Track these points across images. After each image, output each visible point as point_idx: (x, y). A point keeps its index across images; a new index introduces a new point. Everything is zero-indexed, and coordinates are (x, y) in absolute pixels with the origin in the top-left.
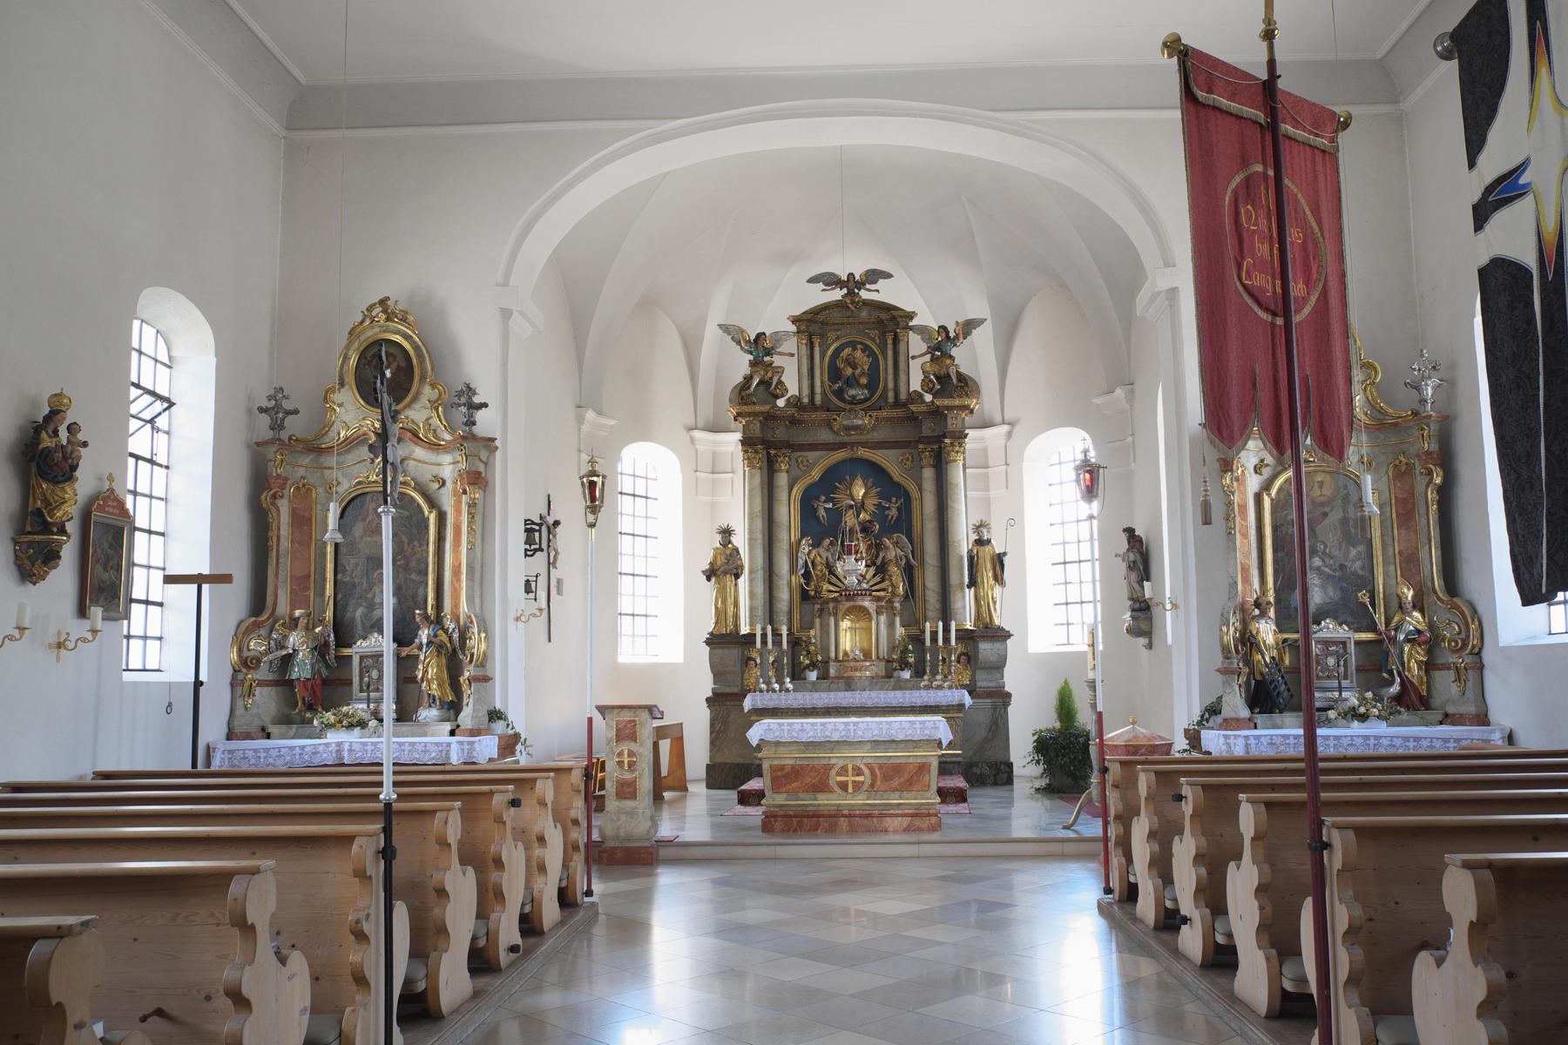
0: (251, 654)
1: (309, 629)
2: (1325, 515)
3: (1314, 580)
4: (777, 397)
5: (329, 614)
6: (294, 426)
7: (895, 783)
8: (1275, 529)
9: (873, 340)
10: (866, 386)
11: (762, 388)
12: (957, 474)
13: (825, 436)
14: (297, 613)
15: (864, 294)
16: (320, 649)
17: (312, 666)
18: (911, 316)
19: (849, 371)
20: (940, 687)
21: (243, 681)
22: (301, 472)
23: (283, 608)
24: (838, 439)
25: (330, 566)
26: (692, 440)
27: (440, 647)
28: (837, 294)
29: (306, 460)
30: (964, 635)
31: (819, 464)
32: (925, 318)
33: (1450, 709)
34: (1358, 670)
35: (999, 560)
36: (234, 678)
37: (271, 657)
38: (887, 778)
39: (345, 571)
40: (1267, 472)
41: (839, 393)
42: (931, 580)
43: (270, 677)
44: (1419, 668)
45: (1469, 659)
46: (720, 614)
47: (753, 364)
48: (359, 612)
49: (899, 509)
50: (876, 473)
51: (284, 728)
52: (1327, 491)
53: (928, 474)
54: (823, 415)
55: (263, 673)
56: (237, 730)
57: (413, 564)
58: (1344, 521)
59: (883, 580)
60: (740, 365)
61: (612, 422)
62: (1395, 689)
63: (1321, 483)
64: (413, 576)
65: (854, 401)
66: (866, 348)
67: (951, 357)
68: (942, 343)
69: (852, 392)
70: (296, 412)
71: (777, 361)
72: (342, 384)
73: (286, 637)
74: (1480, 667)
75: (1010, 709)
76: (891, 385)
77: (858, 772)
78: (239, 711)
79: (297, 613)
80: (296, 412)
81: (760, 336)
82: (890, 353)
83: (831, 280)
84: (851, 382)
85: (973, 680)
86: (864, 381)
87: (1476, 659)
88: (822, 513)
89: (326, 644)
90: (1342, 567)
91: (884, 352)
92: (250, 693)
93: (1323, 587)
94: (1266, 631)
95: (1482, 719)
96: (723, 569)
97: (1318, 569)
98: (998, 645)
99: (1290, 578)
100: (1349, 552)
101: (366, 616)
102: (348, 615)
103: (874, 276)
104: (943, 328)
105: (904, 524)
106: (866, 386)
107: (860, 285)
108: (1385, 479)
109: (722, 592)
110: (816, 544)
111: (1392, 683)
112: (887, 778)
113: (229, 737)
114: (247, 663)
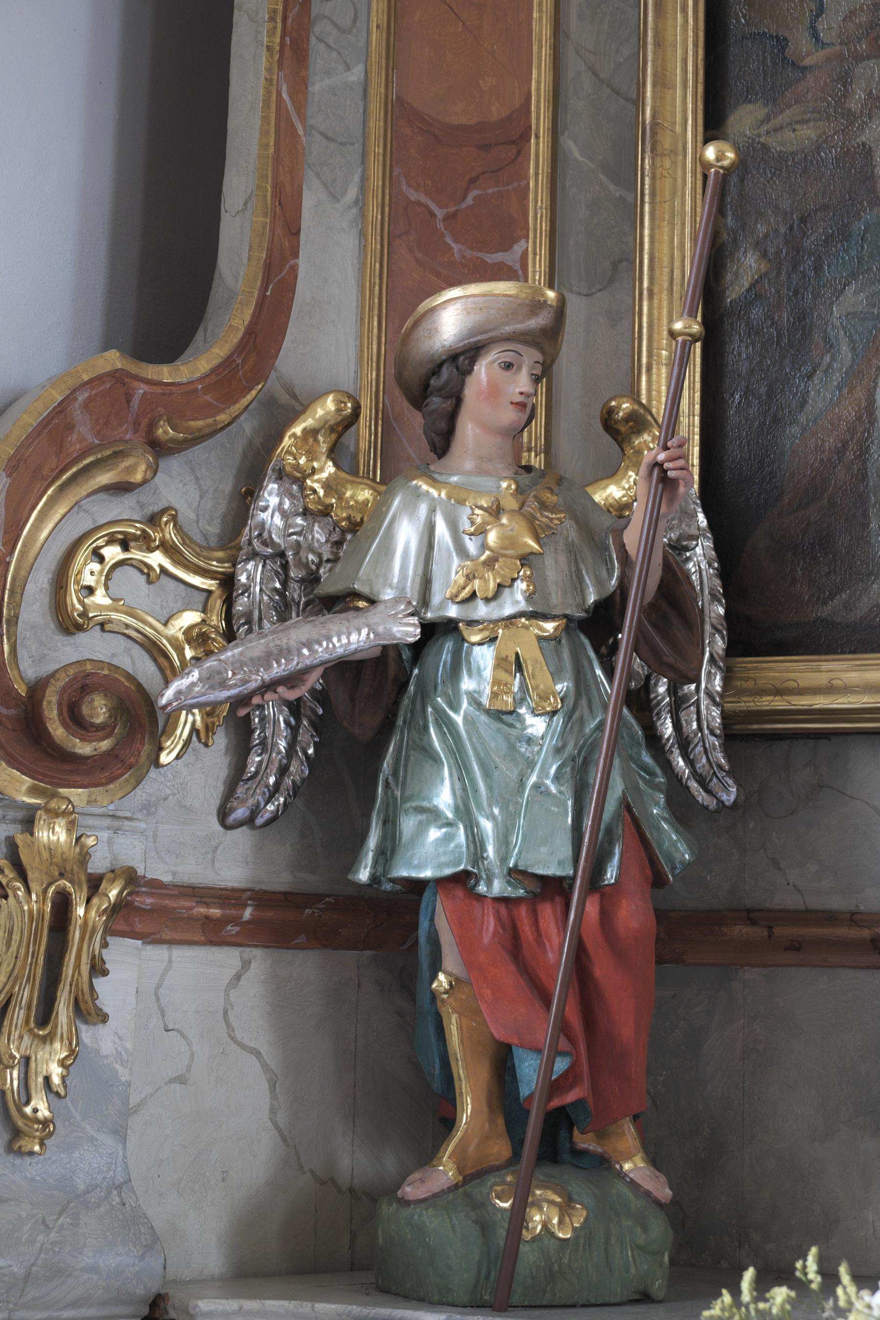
1: (543, 482)
5: (666, 385)
14: (451, 317)
17: (578, 773)
23: (330, 348)
37: (242, 665)
43: (231, 862)
55: (177, 821)
73: (354, 532)
79: (451, 317)
89: (673, 592)
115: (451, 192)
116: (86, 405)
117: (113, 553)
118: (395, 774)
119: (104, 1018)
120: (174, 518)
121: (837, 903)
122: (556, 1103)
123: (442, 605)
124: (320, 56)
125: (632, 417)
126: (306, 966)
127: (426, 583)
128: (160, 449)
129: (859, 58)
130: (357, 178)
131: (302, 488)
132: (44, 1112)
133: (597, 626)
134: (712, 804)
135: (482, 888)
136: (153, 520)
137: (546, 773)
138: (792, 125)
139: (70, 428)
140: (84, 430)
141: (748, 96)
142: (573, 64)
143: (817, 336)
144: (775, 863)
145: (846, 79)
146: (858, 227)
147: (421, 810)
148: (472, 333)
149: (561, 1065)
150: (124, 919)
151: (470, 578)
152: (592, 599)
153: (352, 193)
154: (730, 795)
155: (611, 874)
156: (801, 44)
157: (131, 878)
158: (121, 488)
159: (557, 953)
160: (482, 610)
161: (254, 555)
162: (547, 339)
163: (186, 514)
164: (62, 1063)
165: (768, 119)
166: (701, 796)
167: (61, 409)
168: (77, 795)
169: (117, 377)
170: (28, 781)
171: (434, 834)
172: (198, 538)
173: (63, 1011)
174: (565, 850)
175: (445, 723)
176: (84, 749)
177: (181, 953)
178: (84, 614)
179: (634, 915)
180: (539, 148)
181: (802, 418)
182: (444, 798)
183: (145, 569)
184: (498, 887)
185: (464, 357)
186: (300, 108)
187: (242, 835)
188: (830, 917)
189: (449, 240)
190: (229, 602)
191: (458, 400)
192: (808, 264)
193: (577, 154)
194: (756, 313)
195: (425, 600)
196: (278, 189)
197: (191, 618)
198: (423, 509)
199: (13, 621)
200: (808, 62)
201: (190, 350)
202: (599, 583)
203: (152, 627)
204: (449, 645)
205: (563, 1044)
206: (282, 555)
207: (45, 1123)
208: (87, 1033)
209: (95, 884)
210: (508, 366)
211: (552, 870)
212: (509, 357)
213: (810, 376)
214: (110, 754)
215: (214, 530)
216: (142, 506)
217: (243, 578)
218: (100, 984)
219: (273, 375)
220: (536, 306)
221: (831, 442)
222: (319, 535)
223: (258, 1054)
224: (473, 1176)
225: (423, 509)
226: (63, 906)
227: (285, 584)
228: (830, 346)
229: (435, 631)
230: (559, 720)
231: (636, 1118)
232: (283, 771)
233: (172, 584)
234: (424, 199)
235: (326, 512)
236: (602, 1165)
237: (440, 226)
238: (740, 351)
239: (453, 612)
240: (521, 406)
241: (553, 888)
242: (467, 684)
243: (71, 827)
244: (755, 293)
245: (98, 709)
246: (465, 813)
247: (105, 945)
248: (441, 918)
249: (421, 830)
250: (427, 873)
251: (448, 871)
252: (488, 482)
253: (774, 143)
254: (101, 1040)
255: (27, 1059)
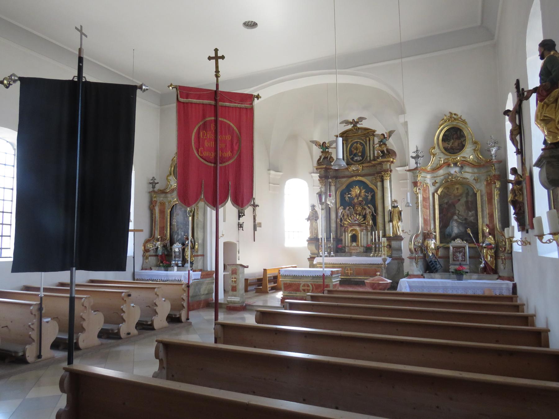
2: (459, 200)
3: (455, 224)
4: (331, 162)
5: (168, 237)
6: (157, 187)
7: (319, 290)
8: (440, 206)
9: (363, 140)
10: (361, 156)
11: (326, 160)
12: (387, 184)
15: (359, 126)
16: (165, 246)
18: (374, 131)
19: (355, 151)
20: (377, 256)
22: (162, 199)
25: (169, 224)
26: (312, 177)
28: (350, 127)
29: (163, 195)
30: (389, 239)
31: (345, 182)
32: (379, 132)
33: (501, 274)
34: (469, 258)
35: (400, 213)
38: (317, 288)
40: (437, 185)
41: (352, 159)
42: (380, 220)
43: (154, 254)
44: (491, 257)
45: (506, 255)
46: (311, 232)
47: (322, 152)
49: (372, 196)
50: (362, 184)
52: (460, 191)
53: (379, 184)
55: (152, 253)
58: (467, 202)
59: (364, 220)
60: (317, 152)
61: (281, 174)
62: (482, 265)
63: (457, 189)
65: (357, 161)
66: (361, 143)
67: (386, 145)
68: (383, 139)
69: (355, 158)
70: (158, 183)
71: (330, 150)
72: (171, 174)
74: (511, 259)
75: (404, 264)
76: (368, 155)
77: (308, 286)
78: (145, 263)
80: (158, 183)
81: (324, 143)
82: (368, 144)
83: (347, 122)
84: (355, 155)
85: (391, 254)
86: (360, 154)
87: (509, 255)
88: (347, 198)
90: (466, 219)
91: (366, 144)
92: (147, 258)
93: (458, 227)
94: (432, 244)
95: (511, 279)
96: (313, 217)
97: (456, 220)
98: (398, 242)
99: (444, 224)
100: (468, 213)
103: (361, 119)
104: (383, 135)
105: (373, 201)
106: (361, 156)
107: (357, 122)
108: (483, 185)
109: (311, 224)
110: (344, 209)
111: (481, 263)
112: (317, 288)
113: (142, 269)
114: (146, 251)
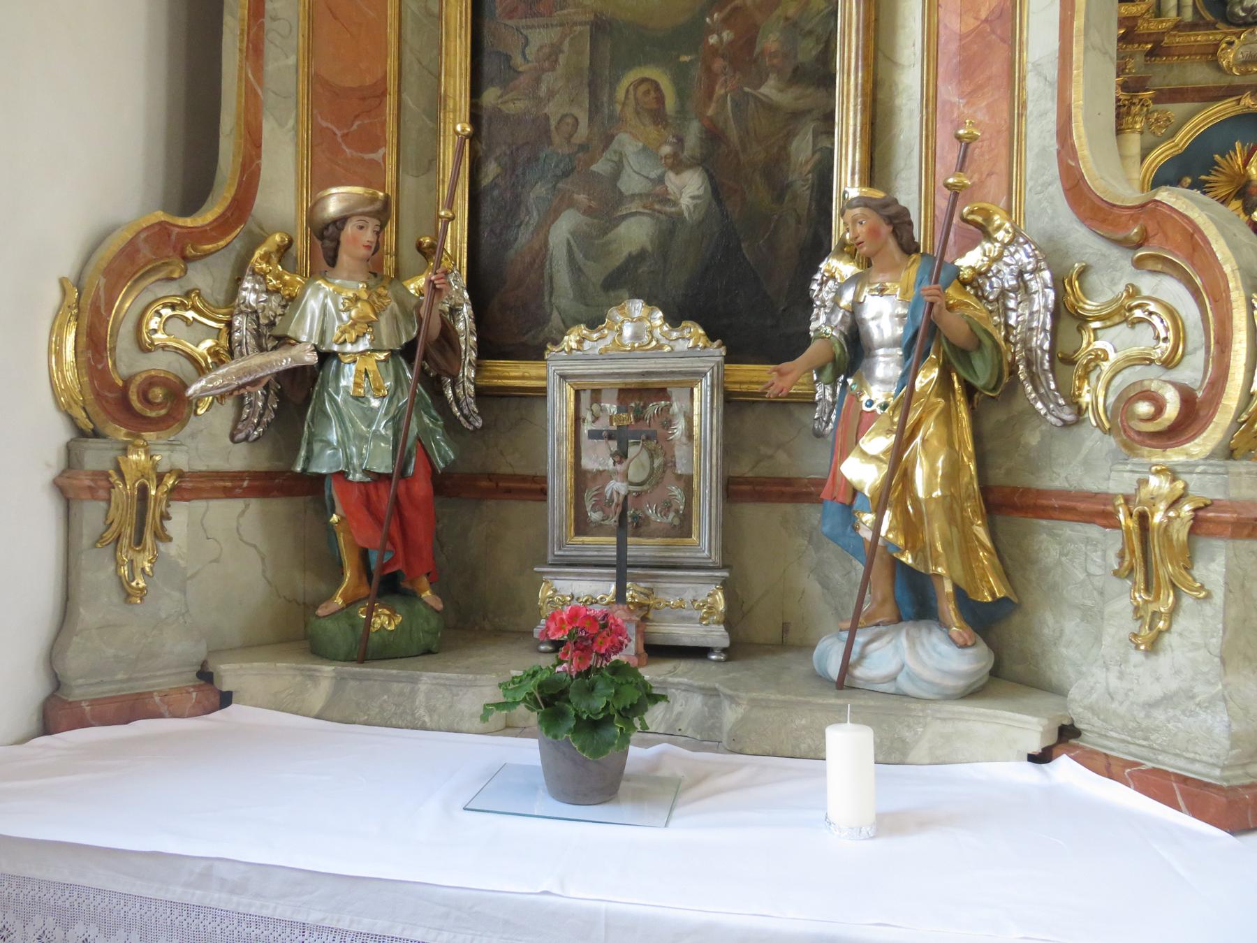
0: (159, 363)
13: (1200, 75)
14: (335, 202)
16: (424, 358)
21: (102, 484)
24: (1224, 81)
27: (956, 358)
36: (71, 457)
39: (509, 73)
43: (238, 459)
48: (563, 229)
51: (283, 673)
54: (1201, 37)
55: (210, 440)
56: (81, 691)
57: (771, 41)
64: (770, 89)
73: (292, 302)
89: (447, 337)
92: (143, 523)
101: (588, 245)
102: (524, 238)
115: (347, 121)
116: (146, 240)
117: (167, 312)
118: (312, 421)
119: (170, 539)
120: (199, 295)
121: (529, 472)
122: (388, 571)
123: (331, 344)
124: (270, 51)
125: (432, 246)
126: (279, 506)
127: (323, 333)
128: (186, 259)
129: (544, 71)
130: (293, 115)
131: (265, 279)
132: (142, 584)
133: (408, 352)
134: (471, 428)
135: (351, 477)
136: (187, 295)
137: (382, 426)
138: (513, 100)
139: (138, 251)
140: (146, 252)
141: (492, 83)
142: (408, 57)
143: (523, 209)
144: (502, 453)
145: (538, 80)
146: (542, 155)
147: (322, 441)
148: (342, 211)
149: (388, 557)
150: (177, 493)
151: (343, 332)
152: (404, 341)
153: (291, 122)
154: (479, 424)
155: (411, 470)
156: (518, 60)
157: (181, 475)
158: (170, 279)
159: (385, 505)
160: (349, 348)
161: (241, 312)
162: (382, 213)
163: (206, 291)
164: (150, 562)
165: (501, 97)
166: (466, 425)
167: (132, 242)
168: (150, 436)
169: (161, 224)
170: (124, 430)
171: (329, 452)
172: (212, 302)
173: (149, 538)
174: (389, 461)
175: (333, 400)
176: (152, 414)
177: (214, 504)
178: (152, 343)
179: (422, 488)
180: (391, 100)
181: (516, 246)
182: (334, 436)
183: (185, 319)
184: (358, 477)
185: (340, 222)
186: (260, 80)
187: (243, 447)
188: (524, 479)
189: (344, 147)
190: (230, 334)
191: (338, 243)
192: (519, 171)
193: (410, 103)
194: (496, 193)
195: (322, 341)
196: (248, 125)
197: (209, 343)
198: (321, 295)
199: (113, 349)
200: (520, 69)
201: (204, 207)
202: (408, 333)
203: (189, 347)
204: (335, 362)
205: (389, 546)
206: (256, 312)
207: (142, 590)
208: (162, 547)
209: (160, 478)
210: (361, 228)
211: (382, 470)
212: (361, 223)
213: (519, 226)
214: (168, 415)
215: (221, 297)
216: (181, 287)
217: (237, 323)
218: (167, 524)
219: (250, 219)
220: (373, 199)
221: (528, 259)
222: (275, 301)
223: (255, 546)
224: (351, 603)
225: (321, 295)
226: (143, 490)
227: (259, 325)
228: (528, 212)
229: (325, 357)
230: (386, 400)
231: (428, 574)
232: (261, 416)
233: (200, 326)
234: (330, 126)
235: (277, 291)
236: (412, 596)
237: (340, 140)
238: (487, 212)
239: (336, 348)
240: (368, 247)
241: (387, 477)
242: (343, 383)
243: (146, 453)
244: (494, 185)
245: (158, 393)
246: (343, 444)
247: (168, 506)
248: (333, 490)
249: (322, 450)
250: (324, 471)
251: (334, 470)
252: (352, 284)
253: (503, 108)
254: (171, 549)
255: (131, 561)
